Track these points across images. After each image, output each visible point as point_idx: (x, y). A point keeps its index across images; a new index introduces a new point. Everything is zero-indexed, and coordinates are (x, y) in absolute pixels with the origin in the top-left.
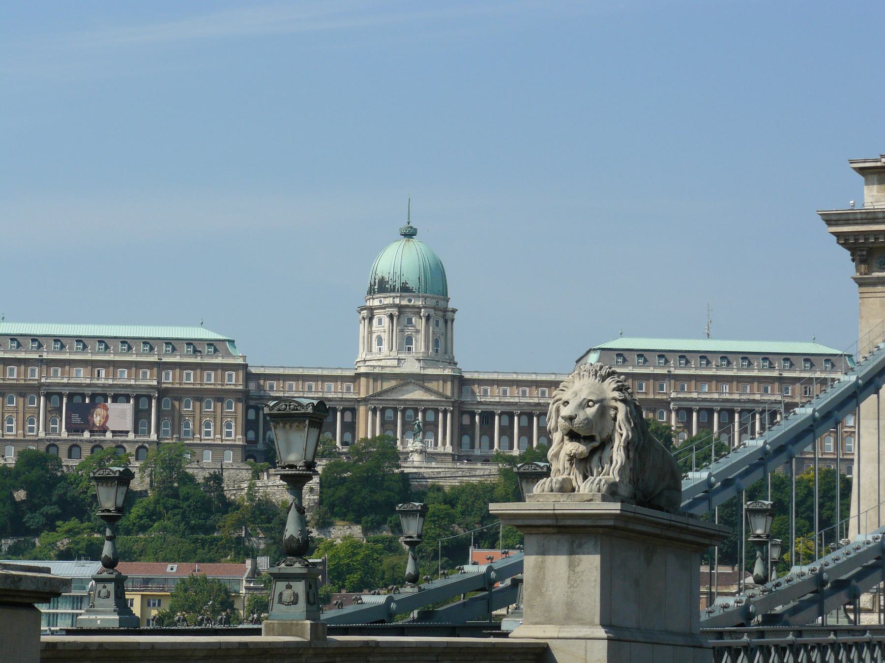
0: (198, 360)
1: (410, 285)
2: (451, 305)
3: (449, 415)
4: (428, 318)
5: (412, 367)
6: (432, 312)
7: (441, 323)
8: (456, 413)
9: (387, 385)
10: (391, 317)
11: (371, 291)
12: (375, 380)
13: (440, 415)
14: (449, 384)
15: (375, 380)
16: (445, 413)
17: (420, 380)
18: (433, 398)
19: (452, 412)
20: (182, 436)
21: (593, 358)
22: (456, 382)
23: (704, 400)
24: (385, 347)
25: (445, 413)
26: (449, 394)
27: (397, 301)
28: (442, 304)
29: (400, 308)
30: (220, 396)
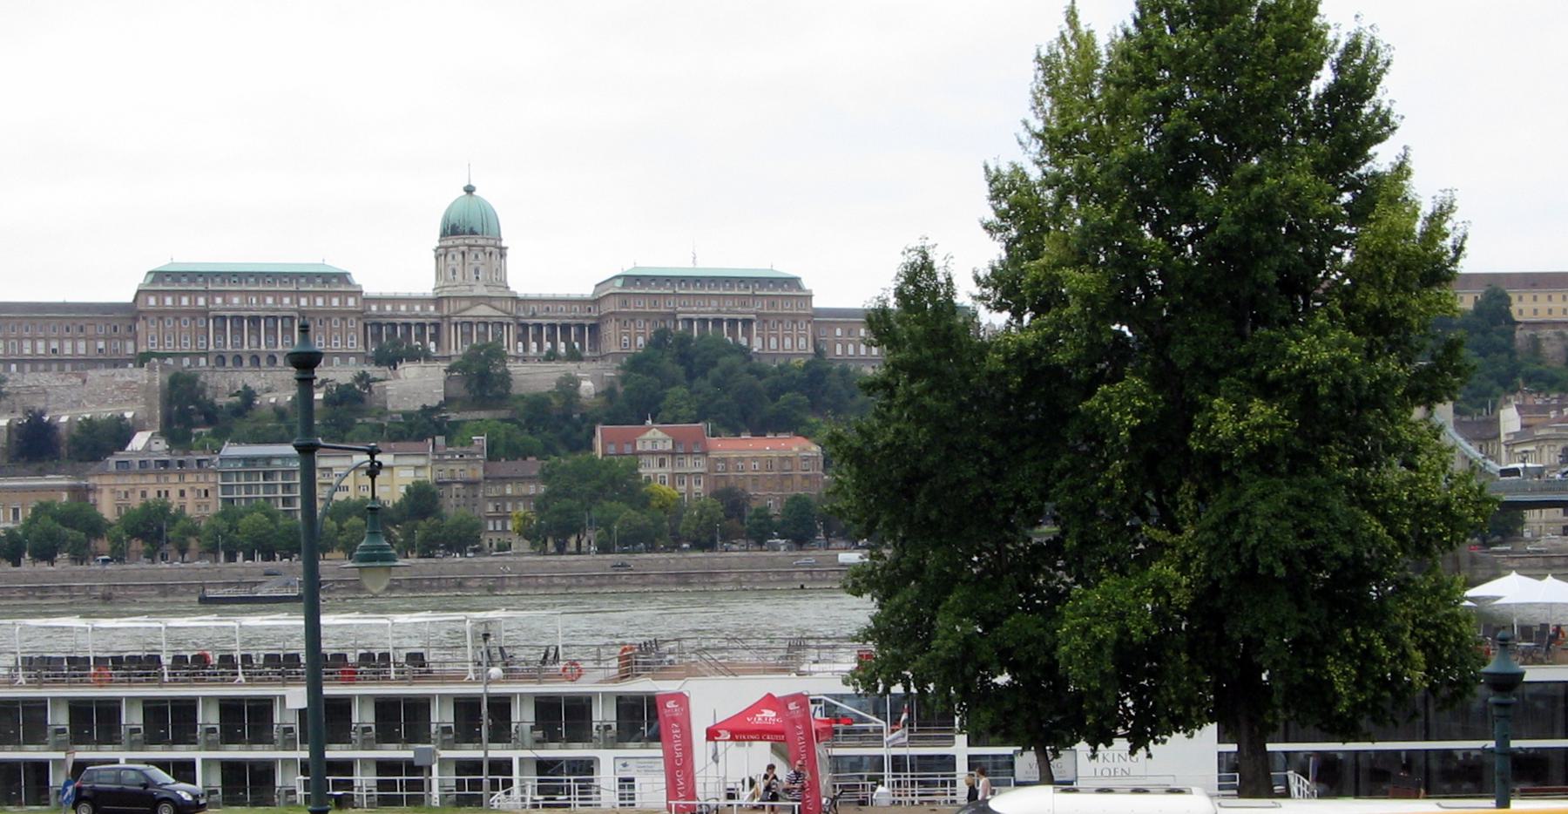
0: (327, 288)
1: (478, 228)
2: (504, 244)
5: (480, 290)
9: (465, 304)
11: (444, 234)
21: (619, 283)
24: (459, 276)
29: (470, 246)
30: (344, 315)
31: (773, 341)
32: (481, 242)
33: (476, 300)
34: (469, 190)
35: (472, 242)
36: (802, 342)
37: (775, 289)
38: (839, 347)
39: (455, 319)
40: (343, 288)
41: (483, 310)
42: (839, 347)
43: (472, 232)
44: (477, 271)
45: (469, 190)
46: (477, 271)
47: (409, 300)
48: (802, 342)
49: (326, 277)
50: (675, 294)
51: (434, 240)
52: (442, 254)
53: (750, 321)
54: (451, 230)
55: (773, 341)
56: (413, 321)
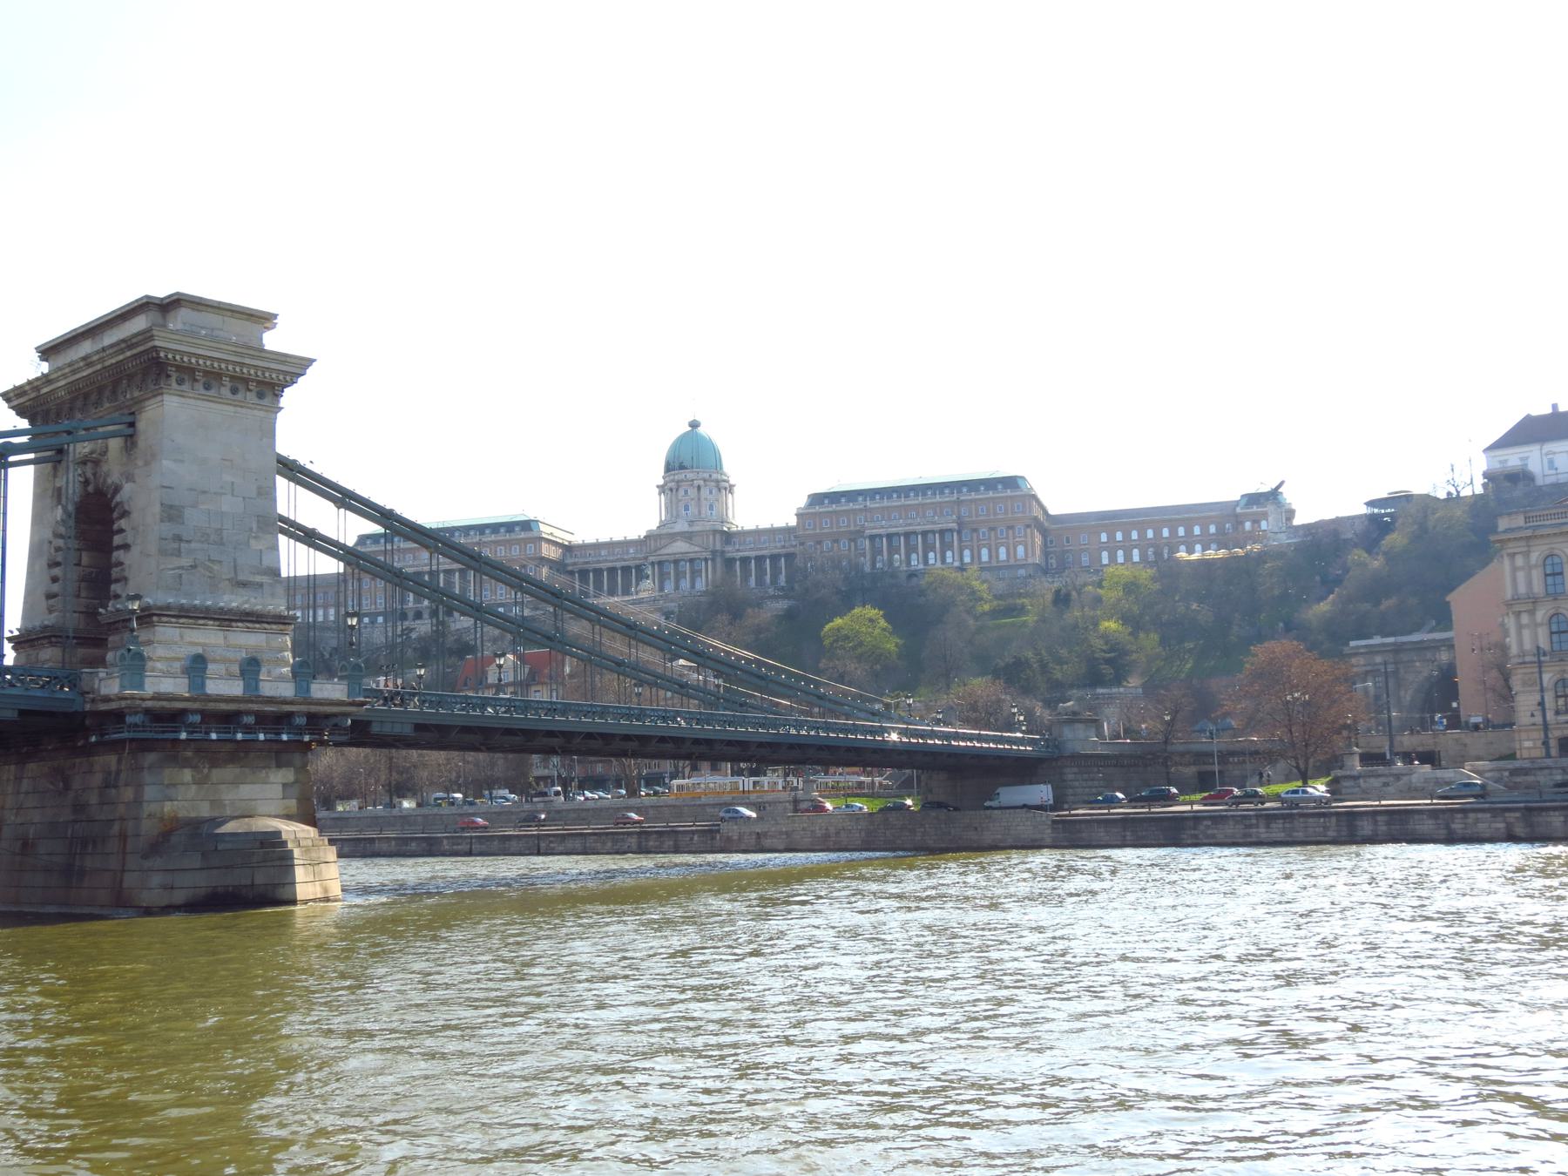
5: (681, 526)
8: (719, 560)
17: (688, 536)
19: (713, 560)
28: (714, 476)
32: (690, 476)
33: (673, 537)
34: (694, 425)
37: (987, 489)
38: (1105, 555)
39: (651, 559)
40: (523, 535)
41: (680, 547)
42: (1105, 555)
43: (682, 467)
44: (686, 508)
45: (694, 425)
46: (686, 508)
47: (626, 544)
49: (510, 527)
50: (866, 509)
51: (658, 475)
52: (662, 489)
53: (951, 530)
54: (669, 468)
56: (619, 564)
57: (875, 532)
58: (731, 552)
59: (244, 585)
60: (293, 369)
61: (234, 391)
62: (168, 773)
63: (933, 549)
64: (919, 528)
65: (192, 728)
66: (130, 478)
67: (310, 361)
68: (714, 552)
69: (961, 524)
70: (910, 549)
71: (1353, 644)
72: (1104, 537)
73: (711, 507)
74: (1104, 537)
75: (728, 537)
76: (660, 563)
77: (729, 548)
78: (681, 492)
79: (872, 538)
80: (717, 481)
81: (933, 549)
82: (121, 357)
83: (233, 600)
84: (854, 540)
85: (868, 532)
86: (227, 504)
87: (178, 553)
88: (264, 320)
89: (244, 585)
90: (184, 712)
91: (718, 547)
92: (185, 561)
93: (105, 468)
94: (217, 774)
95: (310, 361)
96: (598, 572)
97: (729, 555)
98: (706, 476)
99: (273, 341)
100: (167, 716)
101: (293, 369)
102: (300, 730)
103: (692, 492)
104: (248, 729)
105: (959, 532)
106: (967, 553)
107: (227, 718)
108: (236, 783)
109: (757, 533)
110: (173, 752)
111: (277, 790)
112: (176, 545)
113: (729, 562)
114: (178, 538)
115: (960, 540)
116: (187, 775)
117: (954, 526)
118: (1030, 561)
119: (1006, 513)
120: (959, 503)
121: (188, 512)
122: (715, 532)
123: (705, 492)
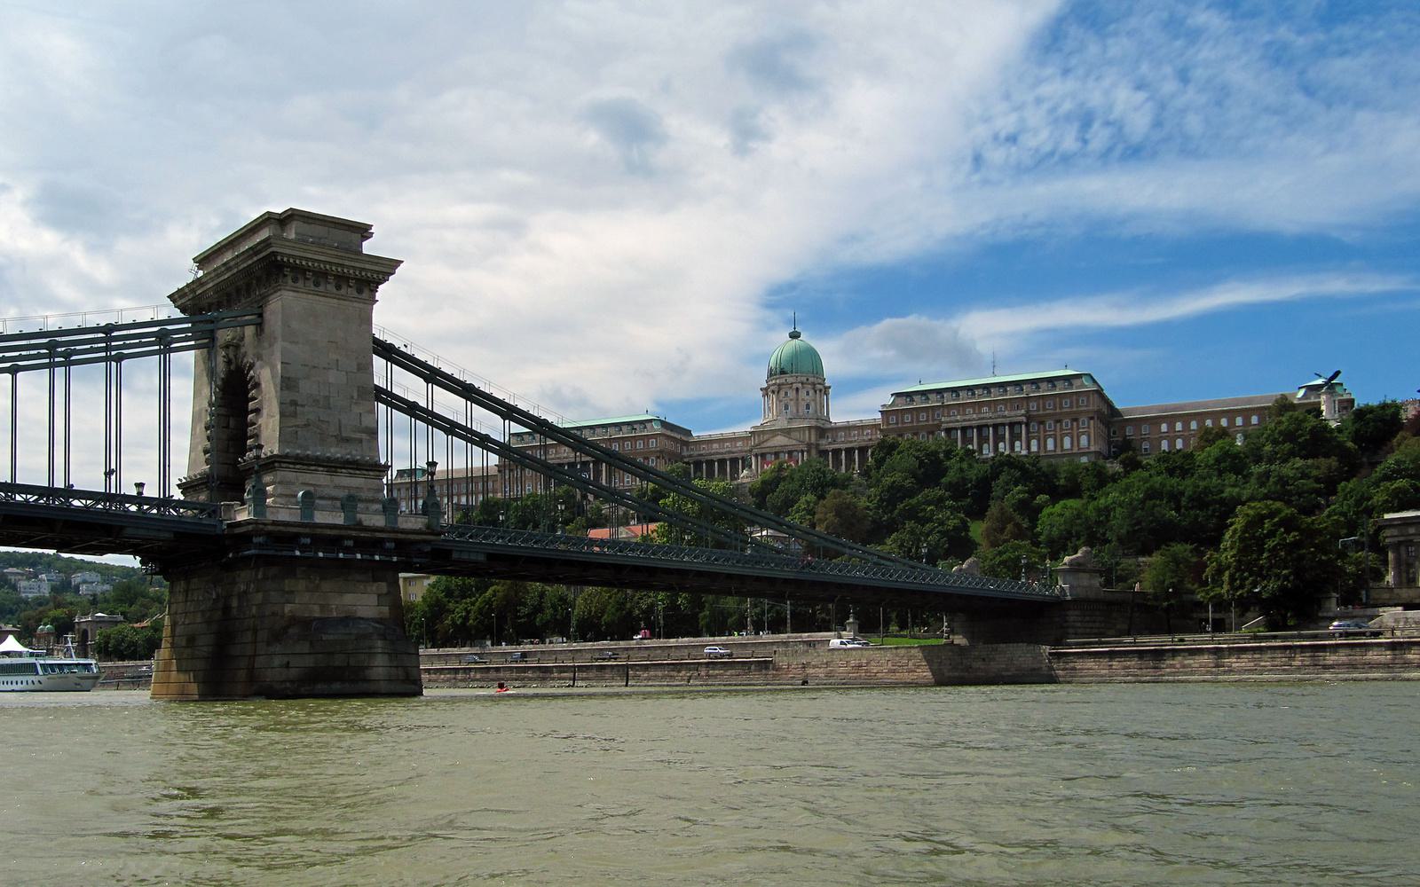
1: (786, 370)
3: (805, 453)
4: (797, 389)
6: (800, 385)
7: (811, 392)
10: (773, 392)
12: (759, 436)
13: (800, 454)
14: (807, 432)
15: (759, 436)
16: (802, 452)
17: (787, 432)
18: (794, 442)
19: (808, 452)
20: (626, 484)
22: (813, 432)
23: (964, 420)
25: (802, 452)
26: (807, 439)
27: (778, 381)
28: (811, 380)
29: (779, 385)
31: (1050, 444)
32: (790, 380)
33: (774, 433)
35: (783, 381)
36: (1084, 440)
39: (755, 451)
41: (780, 440)
43: (783, 372)
44: (786, 408)
46: (786, 408)
48: (1084, 440)
53: (1020, 423)
55: (1050, 444)
56: (727, 456)
57: (951, 425)
58: (825, 444)
59: (347, 440)
60: (386, 268)
61: (338, 287)
62: (288, 584)
63: (1003, 439)
64: (990, 422)
65: (303, 548)
66: (259, 357)
67: (402, 262)
68: (809, 445)
69: (1030, 418)
70: (983, 440)
71: (1387, 516)
72: (1164, 427)
73: (808, 407)
74: (1164, 427)
75: (823, 430)
76: (763, 455)
77: (823, 442)
78: (782, 393)
79: (948, 431)
80: (814, 384)
81: (1003, 439)
82: (250, 262)
83: (336, 452)
84: (932, 433)
85: (944, 426)
86: (333, 377)
87: (295, 415)
88: (364, 231)
89: (347, 440)
90: (297, 535)
91: (813, 440)
92: (300, 421)
93: (243, 350)
94: (326, 586)
95: (402, 262)
96: (710, 463)
97: (822, 448)
98: (804, 379)
99: (368, 247)
100: (283, 537)
101: (386, 268)
102: (389, 553)
103: (792, 394)
104: (347, 550)
105: (1027, 425)
106: (1034, 443)
107: (330, 539)
108: (341, 593)
109: (848, 428)
110: (289, 567)
111: (373, 599)
112: (293, 408)
113: (823, 453)
114: (294, 403)
115: (1028, 432)
116: (302, 585)
117: (1024, 419)
118: (1092, 449)
119: (1071, 407)
120: (1028, 398)
121: (301, 383)
122: (810, 428)
123: (802, 394)
